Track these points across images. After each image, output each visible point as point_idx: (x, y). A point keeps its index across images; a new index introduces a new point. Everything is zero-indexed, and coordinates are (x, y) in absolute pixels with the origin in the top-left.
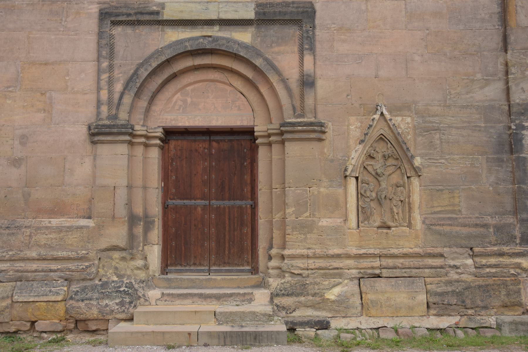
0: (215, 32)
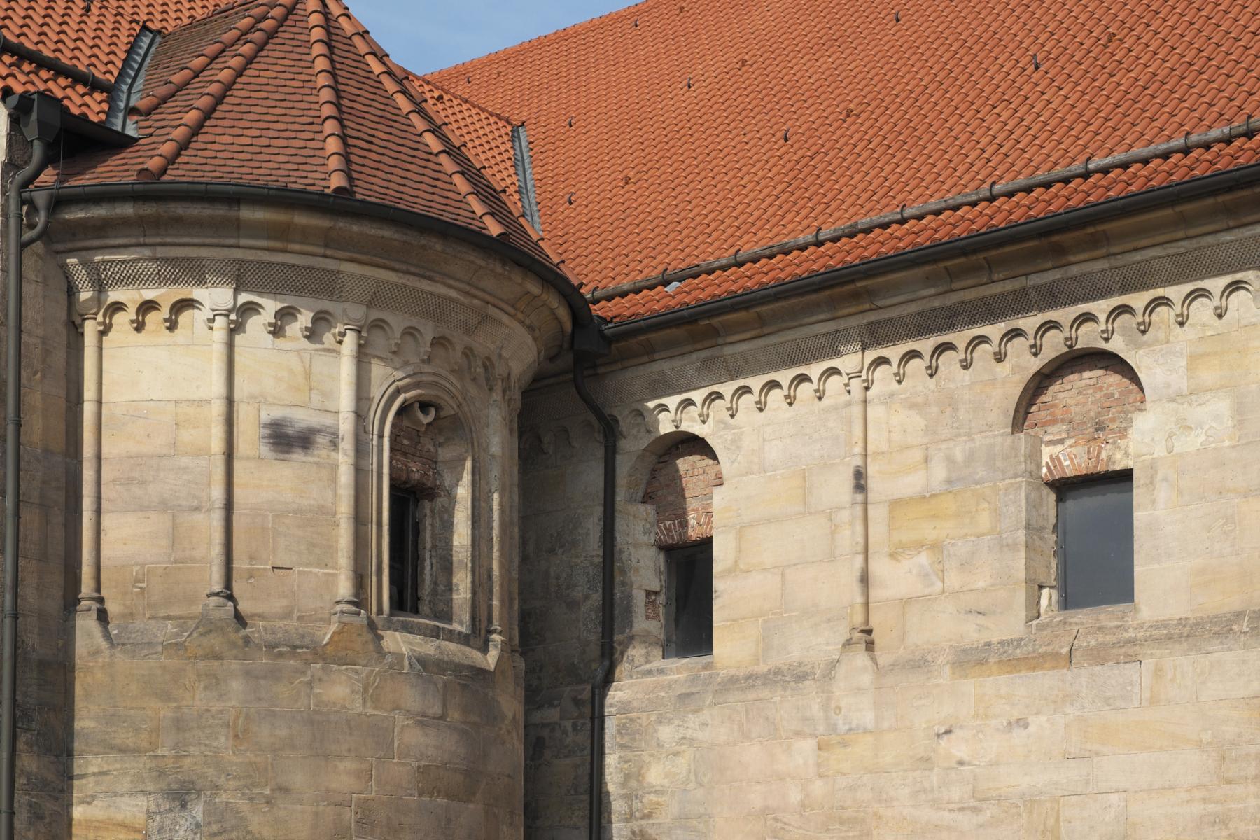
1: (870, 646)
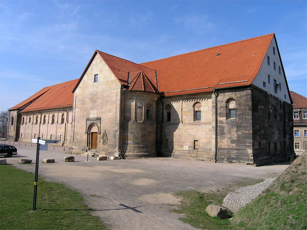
0: (94, 121)
1: (182, 123)
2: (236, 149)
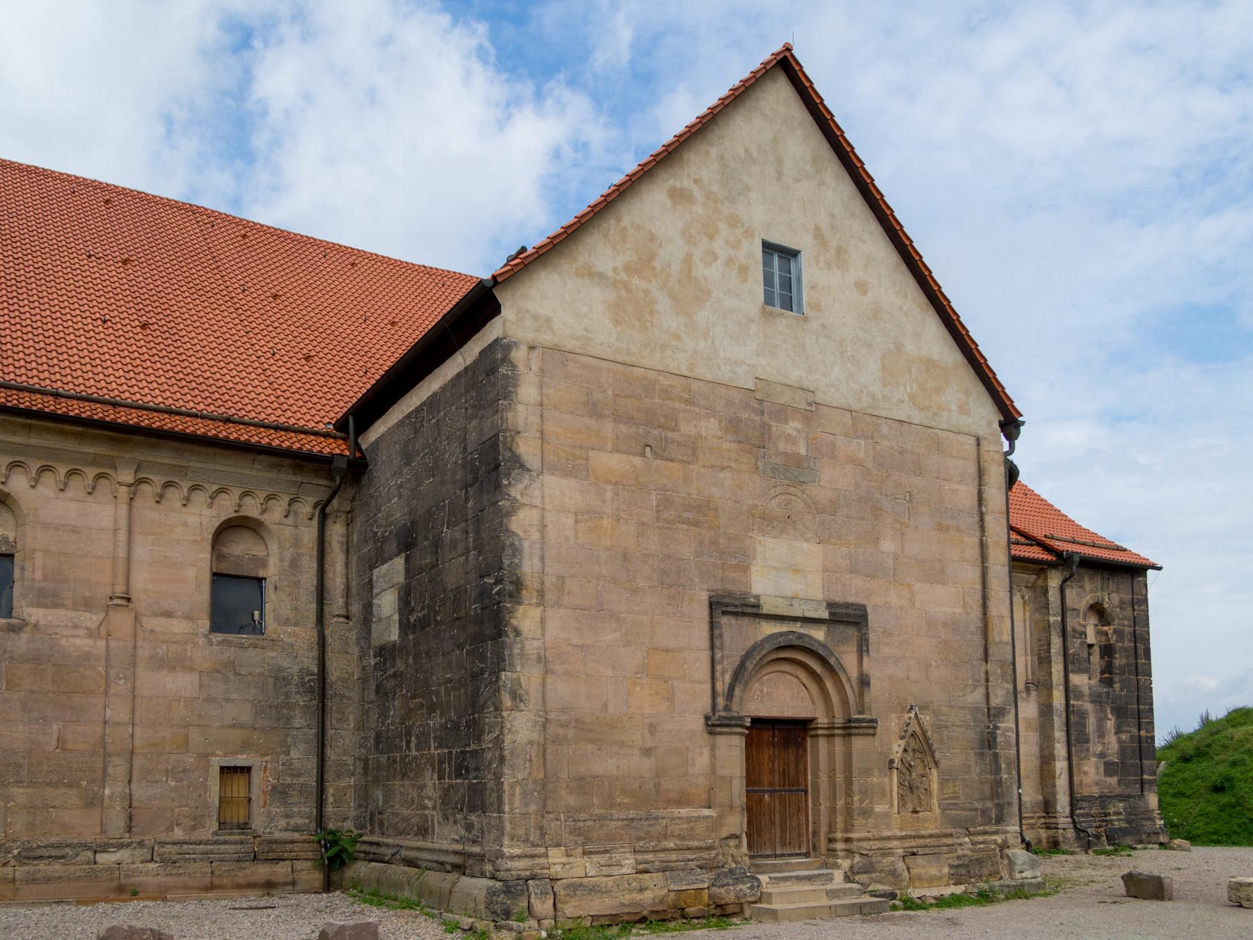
0: (797, 628)
2: (1122, 798)
